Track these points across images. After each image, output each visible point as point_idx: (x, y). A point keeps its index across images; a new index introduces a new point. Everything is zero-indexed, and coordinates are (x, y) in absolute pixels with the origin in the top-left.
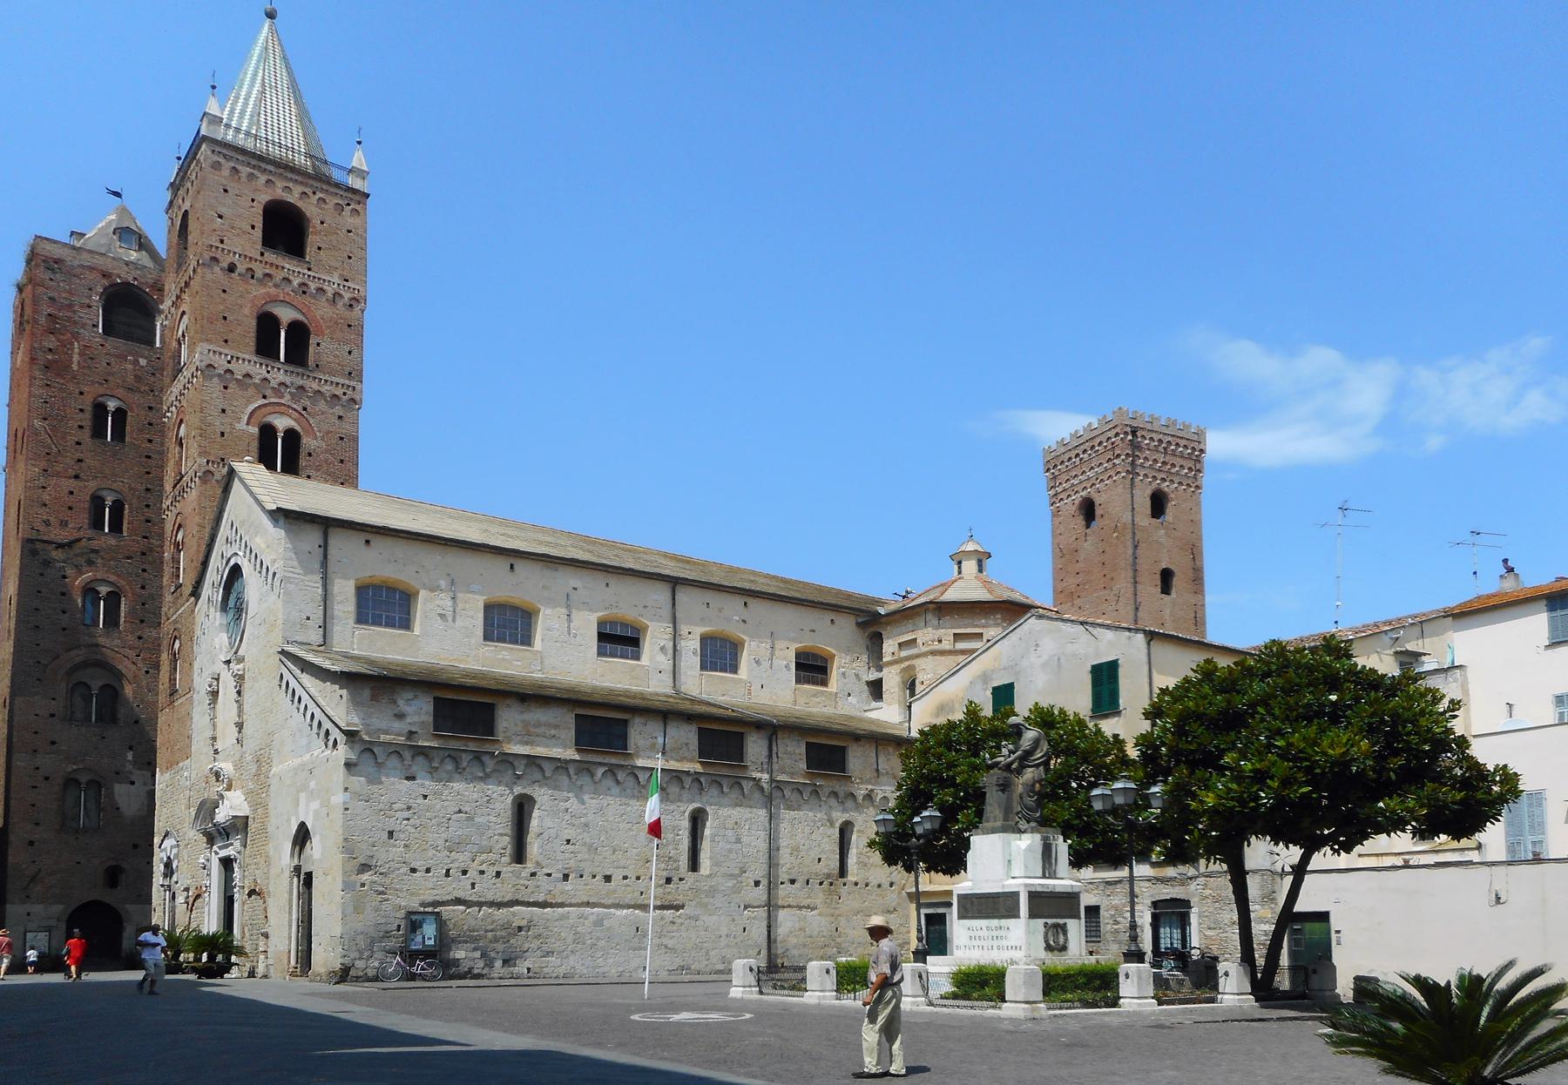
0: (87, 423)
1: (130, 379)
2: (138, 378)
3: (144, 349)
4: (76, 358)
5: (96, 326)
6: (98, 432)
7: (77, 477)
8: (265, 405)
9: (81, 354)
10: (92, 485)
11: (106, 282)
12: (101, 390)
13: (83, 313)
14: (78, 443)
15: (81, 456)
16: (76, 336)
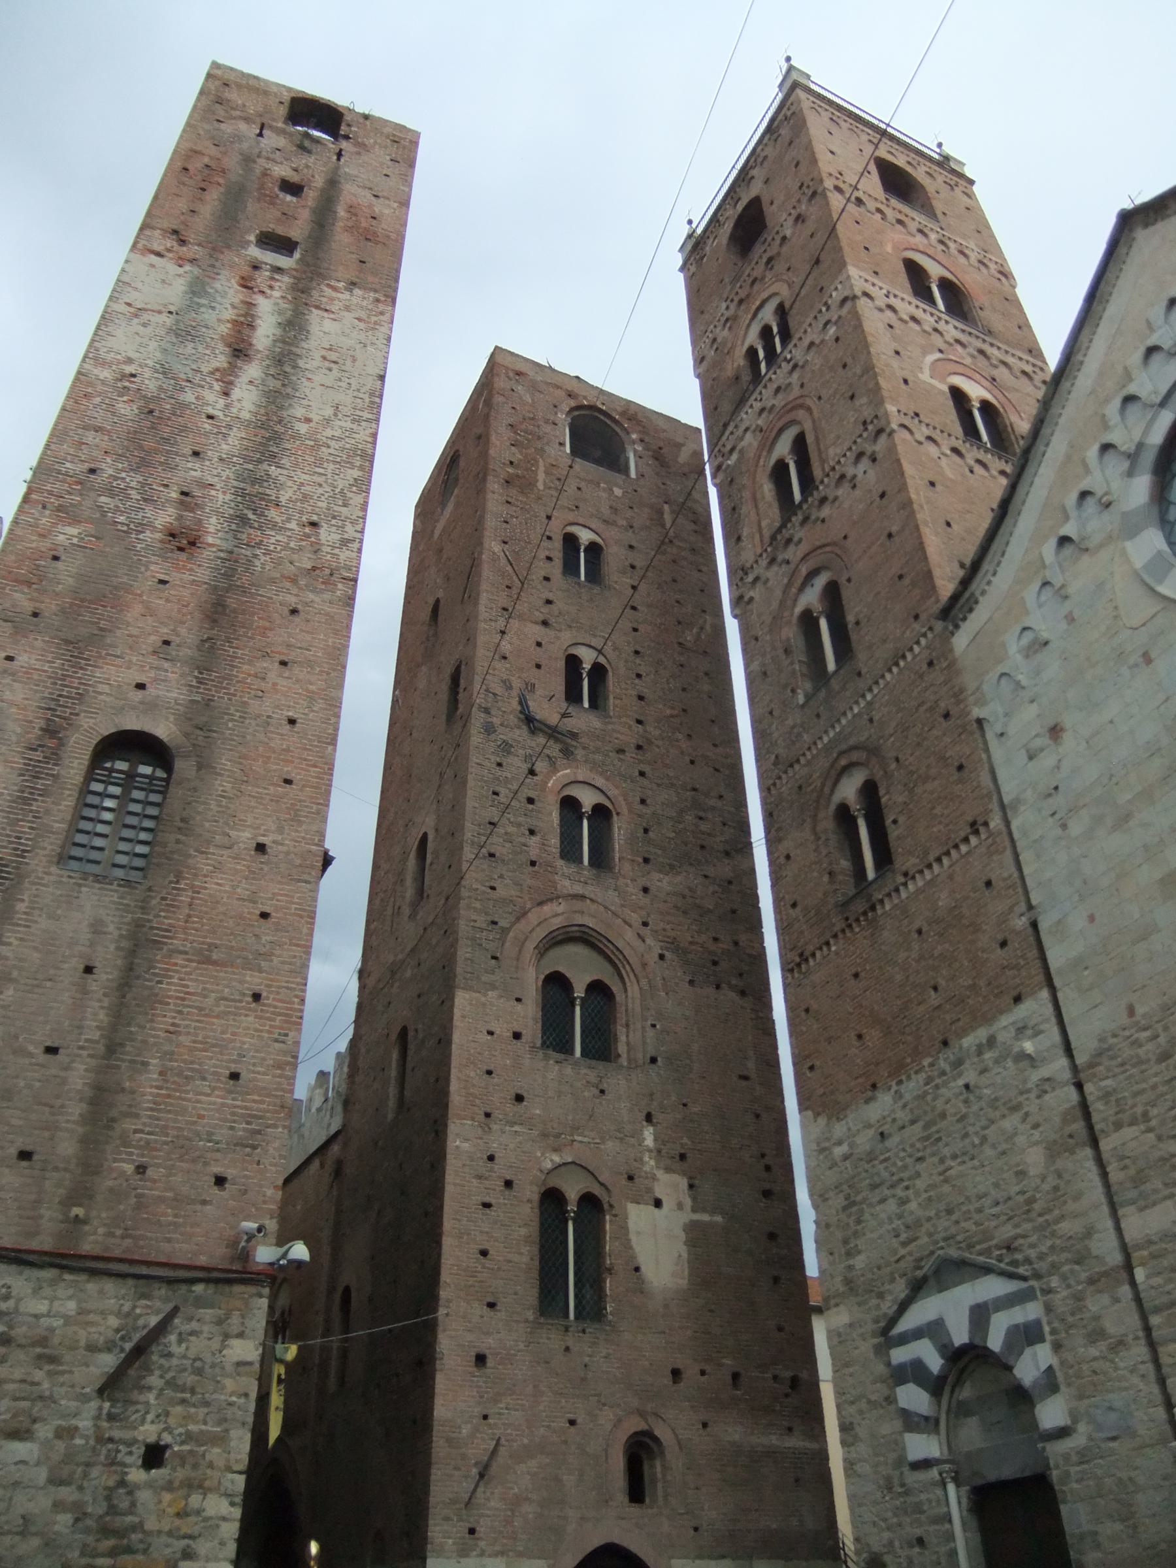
0: (558, 556)
1: (605, 511)
2: (614, 510)
3: (619, 478)
4: (541, 476)
5: (562, 444)
6: (570, 567)
7: (545, 623)
8: (939, 360)
9: (547, 473)
10: (567, 637)
11: (573, 403)
12: (571, 517)
13: (548, 429)
14: (547, 579)
15: (551, 596)
16: (541, 451)
